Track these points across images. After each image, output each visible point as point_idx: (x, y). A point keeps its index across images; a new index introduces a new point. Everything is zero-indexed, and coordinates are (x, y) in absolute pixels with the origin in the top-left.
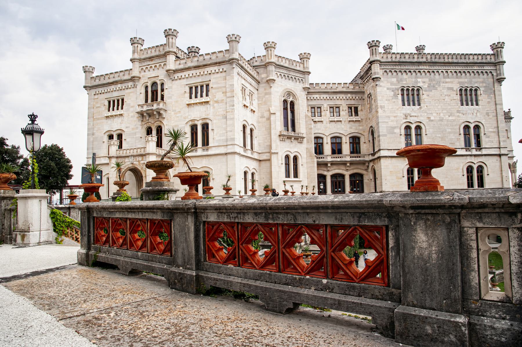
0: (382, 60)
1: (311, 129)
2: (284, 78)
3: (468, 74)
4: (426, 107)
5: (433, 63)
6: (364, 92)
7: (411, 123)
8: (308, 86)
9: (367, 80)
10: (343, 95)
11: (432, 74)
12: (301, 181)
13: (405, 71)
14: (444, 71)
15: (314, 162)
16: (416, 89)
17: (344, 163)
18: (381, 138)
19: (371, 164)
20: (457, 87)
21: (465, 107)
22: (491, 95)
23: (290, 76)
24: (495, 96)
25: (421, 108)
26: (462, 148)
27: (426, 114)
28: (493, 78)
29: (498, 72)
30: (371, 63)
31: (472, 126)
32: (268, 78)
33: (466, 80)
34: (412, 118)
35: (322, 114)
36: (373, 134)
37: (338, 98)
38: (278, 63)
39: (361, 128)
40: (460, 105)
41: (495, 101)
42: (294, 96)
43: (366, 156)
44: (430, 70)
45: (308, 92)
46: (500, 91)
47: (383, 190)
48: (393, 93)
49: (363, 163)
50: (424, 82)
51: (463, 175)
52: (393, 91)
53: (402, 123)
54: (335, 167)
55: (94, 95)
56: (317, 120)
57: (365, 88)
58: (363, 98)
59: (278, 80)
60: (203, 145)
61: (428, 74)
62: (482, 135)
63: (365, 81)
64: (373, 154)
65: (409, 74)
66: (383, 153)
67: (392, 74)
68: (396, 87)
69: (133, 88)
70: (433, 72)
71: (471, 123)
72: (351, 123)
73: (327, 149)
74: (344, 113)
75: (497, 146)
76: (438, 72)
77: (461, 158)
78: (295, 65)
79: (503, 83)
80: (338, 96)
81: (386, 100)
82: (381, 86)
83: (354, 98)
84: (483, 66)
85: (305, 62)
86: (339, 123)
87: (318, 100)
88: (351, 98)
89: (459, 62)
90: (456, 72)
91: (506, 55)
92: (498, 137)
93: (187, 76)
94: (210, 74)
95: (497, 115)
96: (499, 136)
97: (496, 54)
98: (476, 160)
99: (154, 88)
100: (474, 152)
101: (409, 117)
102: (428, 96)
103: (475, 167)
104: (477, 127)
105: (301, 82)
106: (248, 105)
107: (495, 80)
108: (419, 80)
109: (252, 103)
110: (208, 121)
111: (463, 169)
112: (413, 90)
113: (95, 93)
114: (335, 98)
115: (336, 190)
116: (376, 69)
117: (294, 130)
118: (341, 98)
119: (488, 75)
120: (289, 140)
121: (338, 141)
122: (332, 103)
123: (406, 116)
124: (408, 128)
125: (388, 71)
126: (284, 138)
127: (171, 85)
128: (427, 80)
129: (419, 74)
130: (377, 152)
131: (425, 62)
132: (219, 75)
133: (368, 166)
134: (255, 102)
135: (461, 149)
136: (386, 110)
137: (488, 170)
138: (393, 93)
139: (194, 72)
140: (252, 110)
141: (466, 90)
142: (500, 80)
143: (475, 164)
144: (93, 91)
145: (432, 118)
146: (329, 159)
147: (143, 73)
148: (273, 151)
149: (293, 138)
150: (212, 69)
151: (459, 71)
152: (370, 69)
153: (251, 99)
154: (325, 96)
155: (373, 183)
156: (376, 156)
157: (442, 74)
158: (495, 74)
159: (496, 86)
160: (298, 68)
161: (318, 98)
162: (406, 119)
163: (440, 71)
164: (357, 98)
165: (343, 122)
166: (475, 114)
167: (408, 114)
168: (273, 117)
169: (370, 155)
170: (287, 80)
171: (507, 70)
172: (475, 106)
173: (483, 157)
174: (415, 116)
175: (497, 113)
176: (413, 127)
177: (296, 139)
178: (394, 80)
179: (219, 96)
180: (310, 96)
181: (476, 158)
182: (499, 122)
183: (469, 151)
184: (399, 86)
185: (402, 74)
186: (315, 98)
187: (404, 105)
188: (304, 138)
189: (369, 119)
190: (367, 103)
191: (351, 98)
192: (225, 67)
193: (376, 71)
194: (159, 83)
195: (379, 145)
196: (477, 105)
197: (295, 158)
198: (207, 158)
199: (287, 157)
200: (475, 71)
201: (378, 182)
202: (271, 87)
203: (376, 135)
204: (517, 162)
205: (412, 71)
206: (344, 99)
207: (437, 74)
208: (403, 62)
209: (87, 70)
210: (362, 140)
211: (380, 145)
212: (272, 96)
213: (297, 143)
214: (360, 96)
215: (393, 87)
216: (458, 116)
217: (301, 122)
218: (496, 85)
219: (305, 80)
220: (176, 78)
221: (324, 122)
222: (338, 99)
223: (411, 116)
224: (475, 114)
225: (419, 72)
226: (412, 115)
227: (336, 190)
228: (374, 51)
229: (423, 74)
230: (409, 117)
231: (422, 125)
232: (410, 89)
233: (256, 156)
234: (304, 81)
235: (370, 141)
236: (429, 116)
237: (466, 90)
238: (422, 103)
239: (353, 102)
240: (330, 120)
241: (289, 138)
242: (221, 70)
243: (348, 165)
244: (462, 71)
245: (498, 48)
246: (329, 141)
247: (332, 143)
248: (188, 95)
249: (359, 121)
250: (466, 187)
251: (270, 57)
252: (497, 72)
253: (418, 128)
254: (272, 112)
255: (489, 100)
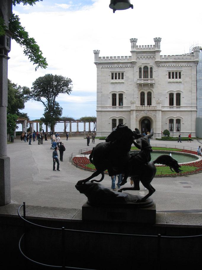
55: (101, 68)
60: (177, 105)
69: (131, 67)
93: (168, 66)
94: (182, 66)
99: (146, 70)
110: (180, 92)
113: (102, 67)
127: (157, 69)
132: (187, 68)
139: (173, 64)
144: (101, 66)
147: (138, 60)
150: (184, 64)
179: (187, 79)
192: (192, 64)
194: (149, 67)
198: (179, 112)
209: (96, 53)
220: (161, 66)
242: (189, 66)
248: (168, 76)
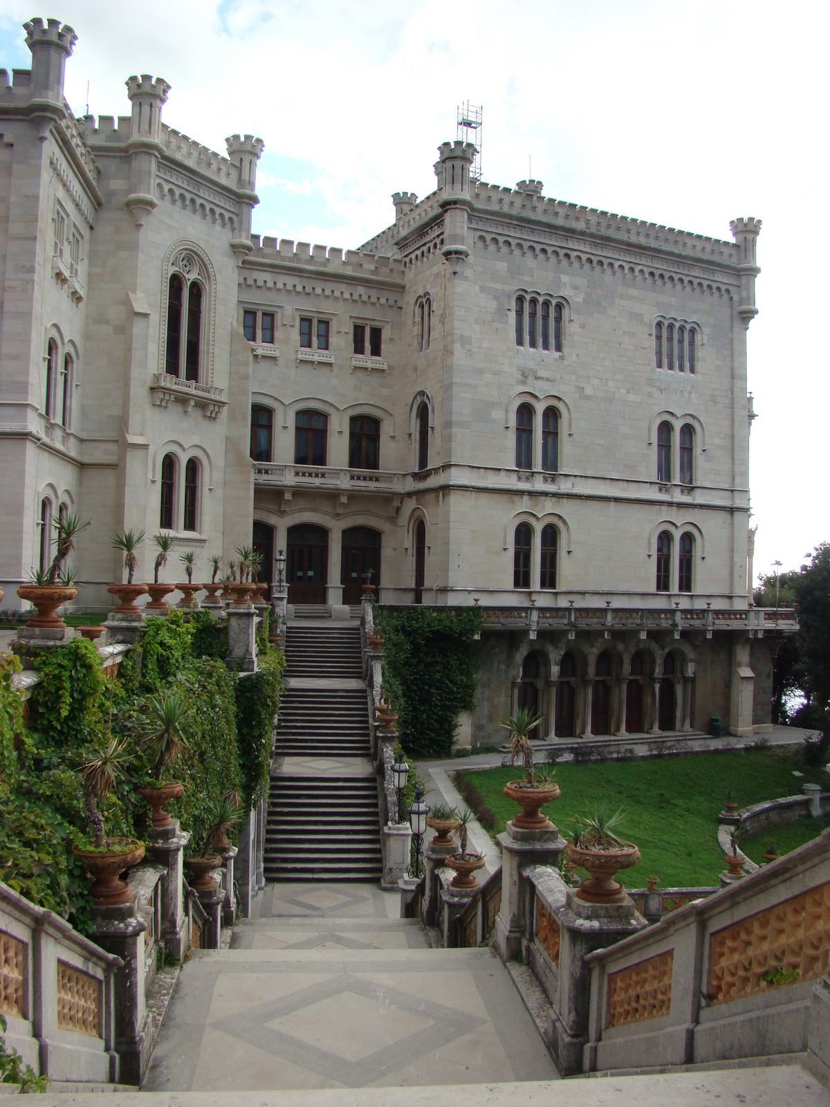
0: (478, 205)
1: (246, 378)
2: (179, 203)
3: (679, 286)
4: (574, 358)
5: (602, 238)
6: (404, 287)
7: (535, 397)
8: (249, 243)
9: (418, 253)
10: (343, 287)
11: (598, 269)
12: (204, 541)
13: (532, 248)
14: (627, 266)
15: (249, 482)
16: (554, 302)
17: (332, 496)
18: (454, 430)
19: (410, 505)
20: (652, 316)
21: (665, 371)
22: (725, 351)
23: (199, 201)
24: (732, 355)
25: (562, 358)
26: (651, 483)
27: (574, 378)
28: (732, 308)
29: (744, 294)
30: (446, 205)
31: (677, 425)
32: (133, 196)
33: (673, 301)
34: (539, 384)
35: (277, 335)
36: (423, 413)
37: (328, 292)
38: (167, 153)
39: (385, 392)
40: (654, 364)
41: (732, 369)
42: (204, 267)
43: (395, 479)
44: (593, 257)
45: (244, 262)
46: (744, 342)
47: (451, 583)
48: (494, 304)
49: (387, 499)
50: (575, 288)
51: (649, 556)
52: (496, 298)
53: (512, 392)
54: (302, 503)
56: (260, 352)
57: (410, 275)
58: (399, 304)
59: (163, 206)
61: (587, 266)
62: (697, 451)
63: (413, 256)
64: (419, 477)
65: (541, 256)
66: (457, 477)
67: (499, 250)
68: (507, 288)
70: (601, 263)
71: (677, 418)
72: (359, 374)
73: (284, 443)
74: (341, 340)
75: (726, 486)
76: (611, 265)
77: (647, 507)
78: (214, 167)
79: (752, 323)
80: (329, 287)
81: (477, 322)
82: (466, 279)
83: (373, 300)
84: (713, 271)
85: (246, 164)
86: (326, 370)
87: (269, 289)
88: (365, 298)
89: (663, 248)
90: (652, 274)
91: (765, 252)
92: (730, 461)
95: (732, 404)
96: (733, 459)
97: (742, 249)
98: (680, 518)
100: (679, 497)
101: (531, 378)
102: (583, 326)
103: (677, 535)
104: (688, 430)
105: (228, 225)
106: (67, 274)
107: (735, 312)
108: (565, 279)
109: (76, 270)
111: (649, 539)
112: (546, 304)
114: (318, 291)
115: (300, 574)
116: (457, 225)
117: (193, 374)
118: (337, 294)
119: (721, 296)
120: (179, 408)
121: (316, 425)
122: (309, 306)
123: (525, 375)
124: (525, 411)
125: (488, 237)
126: (167, 397)
128: (582, 282)
129: (565, 262)
130: (436, 470)
131: (583, 233)
133: (398, 510)
134: (82, 268)
135: (648, 485)
136: (476, 350)
137: (703, 546)
138: (494, 304)
140: (74, 293)
141: (671, 327)
142: (747, 315)
143: (677, 527)
145: (588, 391)
146: (289, 479)
148: (132, 439)
149: (192, 403)
151: (660, 272)
152: (437, 221)
153: (75, 257)
154: (290, 281)
155: (411, 561)
156: (432, 482)
157: (619, 273)
158: (736, 298)
159: (736, 330)
160: (223, 181)
161: (270, 284)
162: (524, 383)
163: (616, 264)
164: (383, 301)
165: (335, 369)
166: (686, 395)
167: (531, 369)
168: (138, 328)
169: (410, 479)
170: (188, 213)
171: (764, 290)
172: (687, 374)
173: (696, 510)
174: (548, 380)
175: (733, 399)
176: (540, 408)
177: (202, 405)
178: (502, 266)
180: (246, 273)
181: (683, 511)
182: (737, 424)
183: (667, 491)
184: (512, 287)
185: (523, 254)
186: (260, 283)
187: (520, 342)
188: (221, 404)
189: (416, 369)
190: (410, 321)
191: (365, 298)
193: (458, 231)
195: (449, 452)
196: (692, 370)
197: (193, 466)
199: (169, 463)
200: (696, 281)
201: (429, 560)
202: (139, 226)
203: (434, 420)
204: (756, 529)
205: (550, 250)
206: (346, 300)
207: (608, 271)
208: (529, 221)
210: (386, 431)
211: (450, 450)
212: (141, 256)
213: (200, 419)
214: (392, 297)
215: (498, 286)
216: (650, 395)
217: (217, 352)
218: (737, 324)
219: (241, 222)
221: (281, 362)
222: (327, 297)
223: (537, 378)
224: (686, 395)
225: (567, 256)
226: (540, 374)
227: (300, 574)
228: (458, 171)
229: (576, 264)
230: (530, 379)
231: (561, 407)
232: (541, 300)
233: (72, 450)
234: (236, 225)
235: (410, 435)
236: (582, 385)
237: (671, 327)
238: (566, 342)
239: (368, 312)
240: (300, 357)
241: (182, 400)
243: (344, 499)
244: (667, 275)
245: (747, 230)
246: (291, 422)
247: (297, 429)
249: (383, 371)
250: (652, 588)
251: (145, 126)
252: (739, 293)
253: (552, 414)
254: (137, 310)
255: (719, 363)
